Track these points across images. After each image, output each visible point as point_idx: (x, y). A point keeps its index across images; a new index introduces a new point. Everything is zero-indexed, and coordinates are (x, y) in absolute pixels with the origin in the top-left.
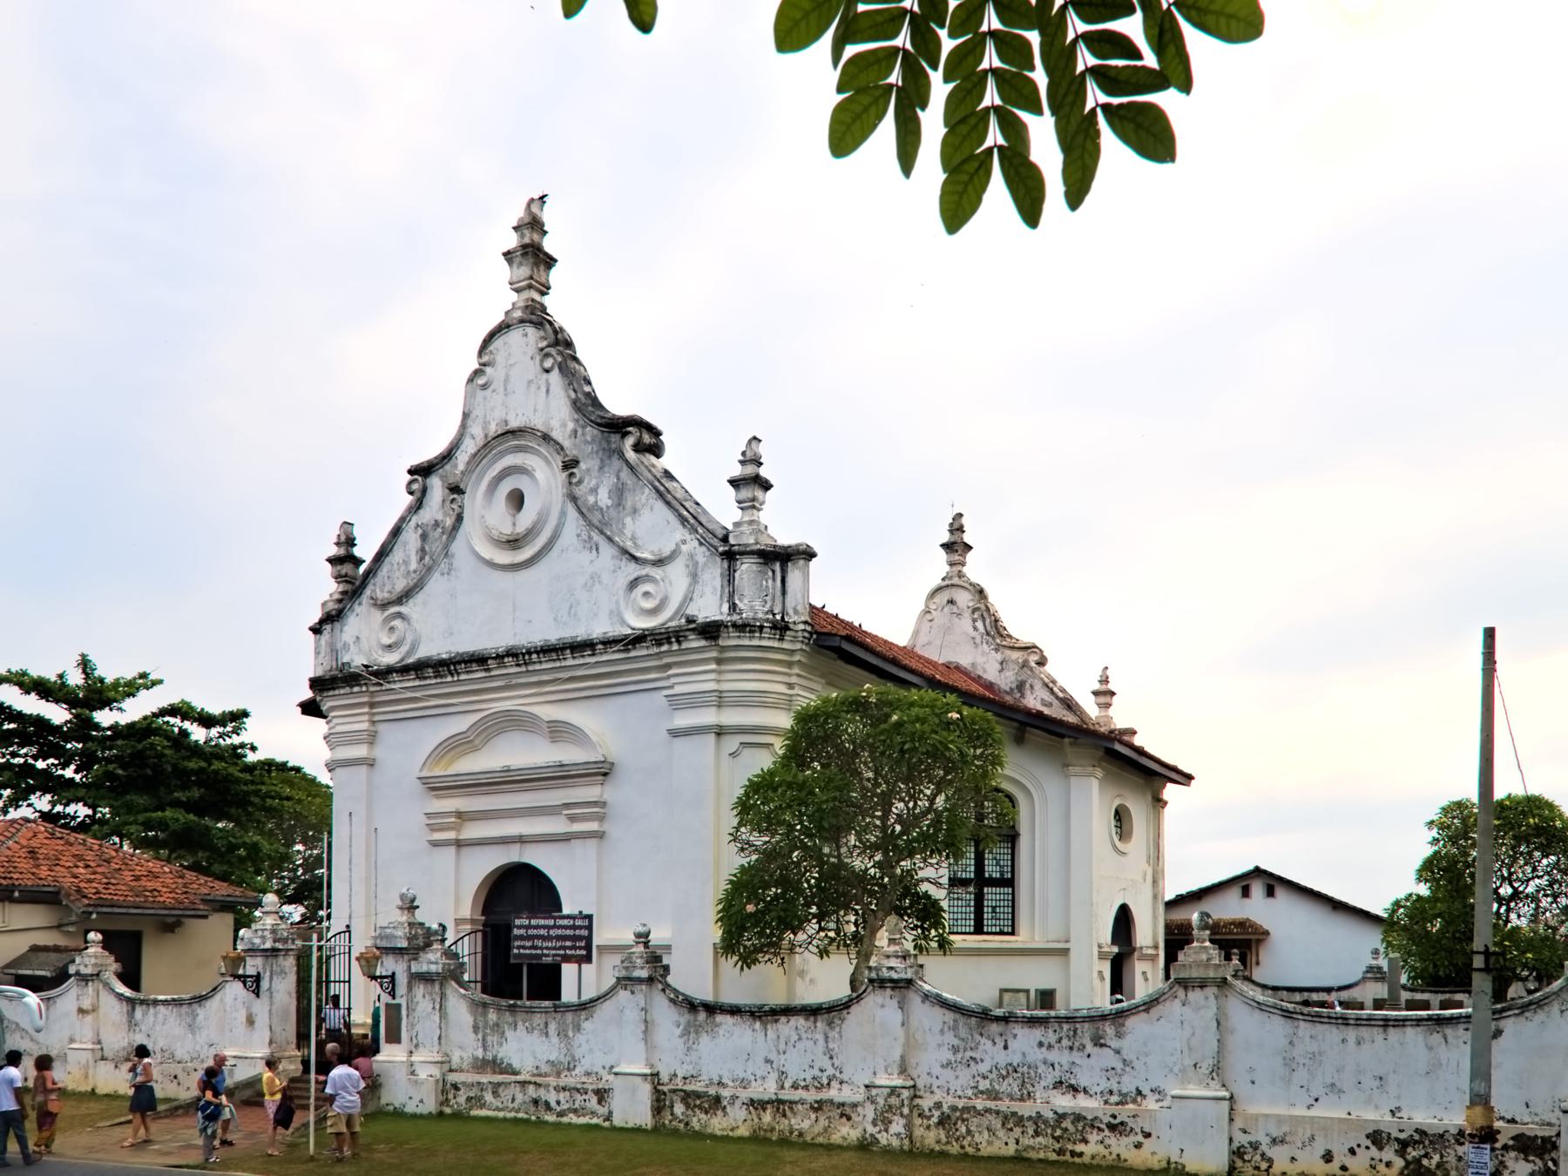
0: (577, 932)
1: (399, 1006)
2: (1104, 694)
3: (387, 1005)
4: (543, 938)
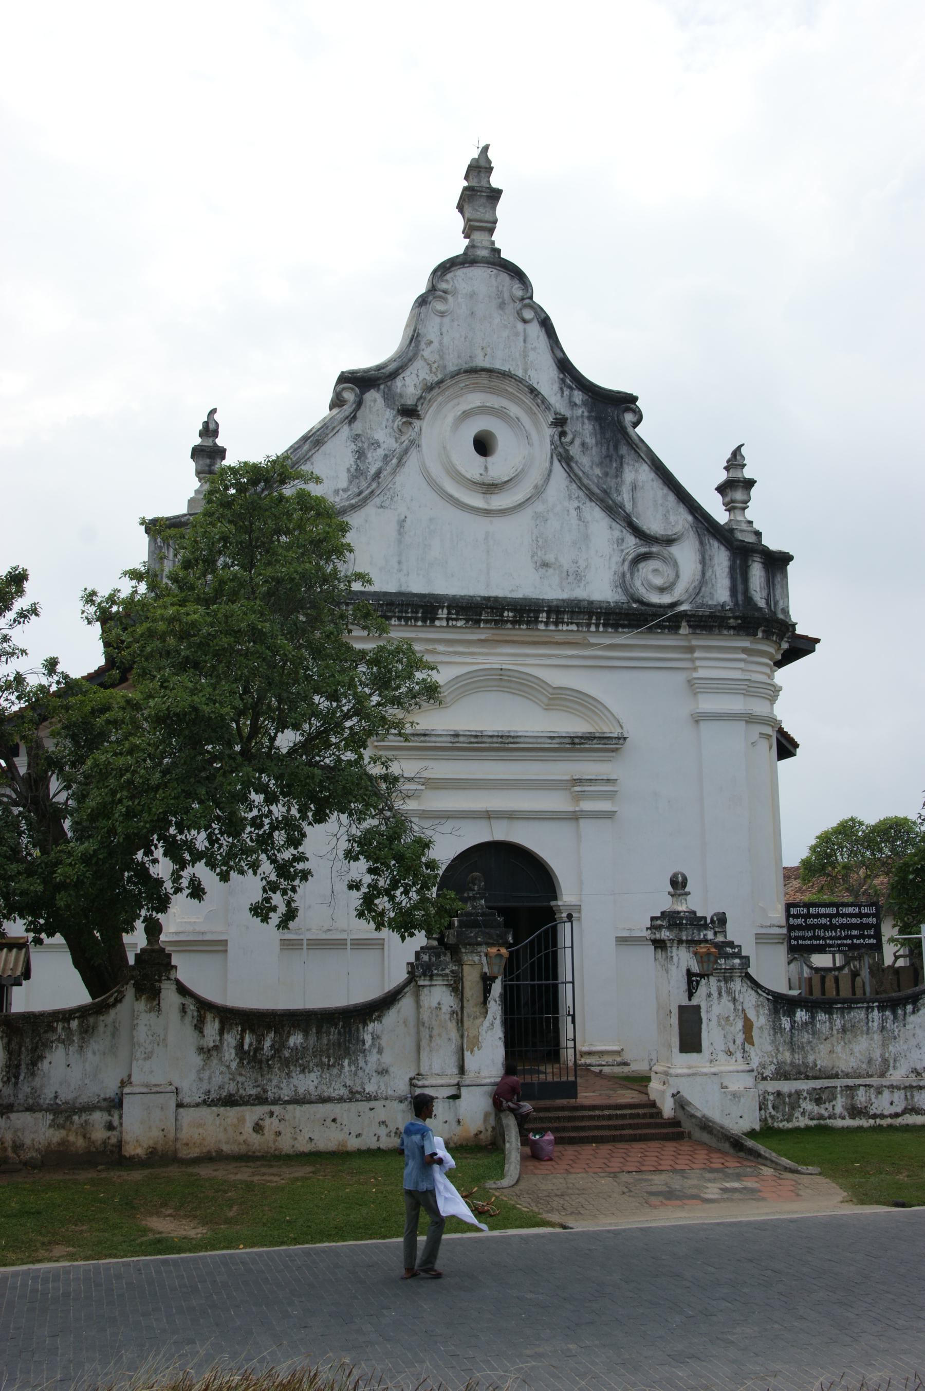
0: (865, 920)
1: (698, 1007)
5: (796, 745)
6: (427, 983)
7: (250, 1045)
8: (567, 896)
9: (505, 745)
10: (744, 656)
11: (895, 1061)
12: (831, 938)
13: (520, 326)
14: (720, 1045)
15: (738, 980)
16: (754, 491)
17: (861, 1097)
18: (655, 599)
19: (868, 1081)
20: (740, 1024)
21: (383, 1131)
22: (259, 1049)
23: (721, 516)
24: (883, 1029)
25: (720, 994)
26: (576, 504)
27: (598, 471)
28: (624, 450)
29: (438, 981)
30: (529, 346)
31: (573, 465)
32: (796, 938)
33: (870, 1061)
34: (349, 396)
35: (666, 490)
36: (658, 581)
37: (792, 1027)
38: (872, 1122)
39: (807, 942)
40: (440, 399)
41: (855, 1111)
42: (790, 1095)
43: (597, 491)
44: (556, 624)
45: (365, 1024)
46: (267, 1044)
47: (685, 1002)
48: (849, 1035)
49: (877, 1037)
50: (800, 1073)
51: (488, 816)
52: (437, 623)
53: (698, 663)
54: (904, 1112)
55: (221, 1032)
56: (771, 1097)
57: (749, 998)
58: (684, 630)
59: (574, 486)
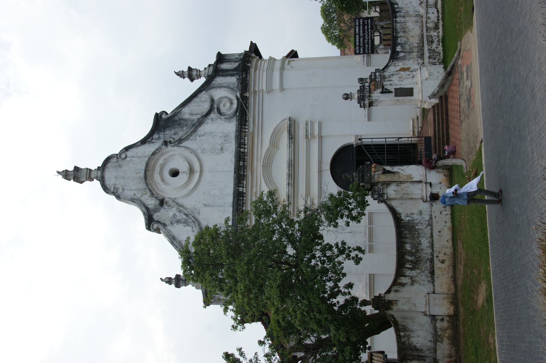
0: (361, 24)
1: (395, 89)
4: (364, 39)
5: (293, 51)
6: (386, 195)
7: (410, 265)
8: (352, 140)
9: (292, 165)
10: (258, 71)
11: (416, 12)
12: (368, 37)
13: (128, 159)
14: (410, 81)
15: (385, 73)
16: (193, 67)
17: (431, 25)
18: (235, 106)
19: (424, 22)
20: (402, 73)
21: (444, 213)
22: (412, 261)
23: (203, 80)
24: (404, 17)
25: (390, 80)
26: (198, 137)
27: (185, 128)
28: (177, 118)
29: (385, 191)
30: (136, 155)
31: (182, 138)
32: (368, 50)
33: (417, 22)
34: (156, 226)
35: (192, 102)
36: (228, 105)
37: (403, 52)
38: (440, 21)
39: (370, 46)
40: (157, 190)
41: (436, 28)
42: (430, 53)
43: (193, 129)
44: (245, 145)
45: (402, 220)
46: (410, 258)
47: (393, 94)
48: (406, 30)
49: (407, 19)
50: (421, 49)
51: (320, 171)
52: (245, 191)
53: (260, 89)
54: (437, 8)
55: (405, 276)
56: (431, 60)
57: (392, 69)
58: (247, 94)
59: (191, 138)
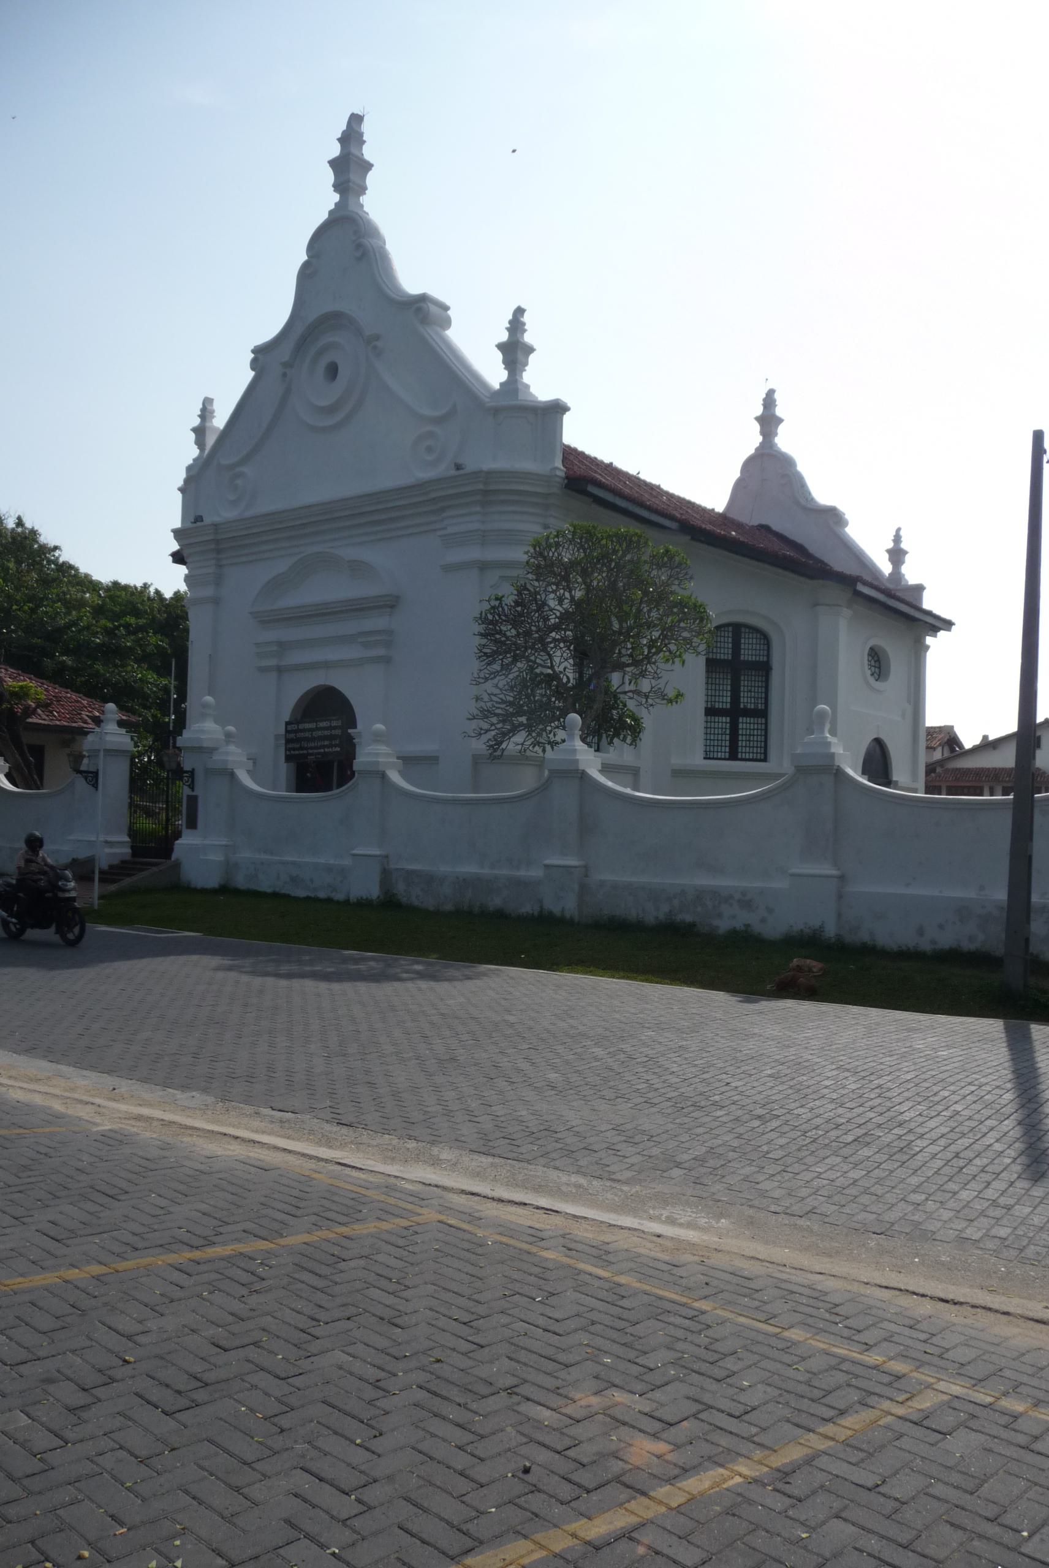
0: (334, 732)
2: (897, 555)
3: (188, 796)
12: (312, 748)
